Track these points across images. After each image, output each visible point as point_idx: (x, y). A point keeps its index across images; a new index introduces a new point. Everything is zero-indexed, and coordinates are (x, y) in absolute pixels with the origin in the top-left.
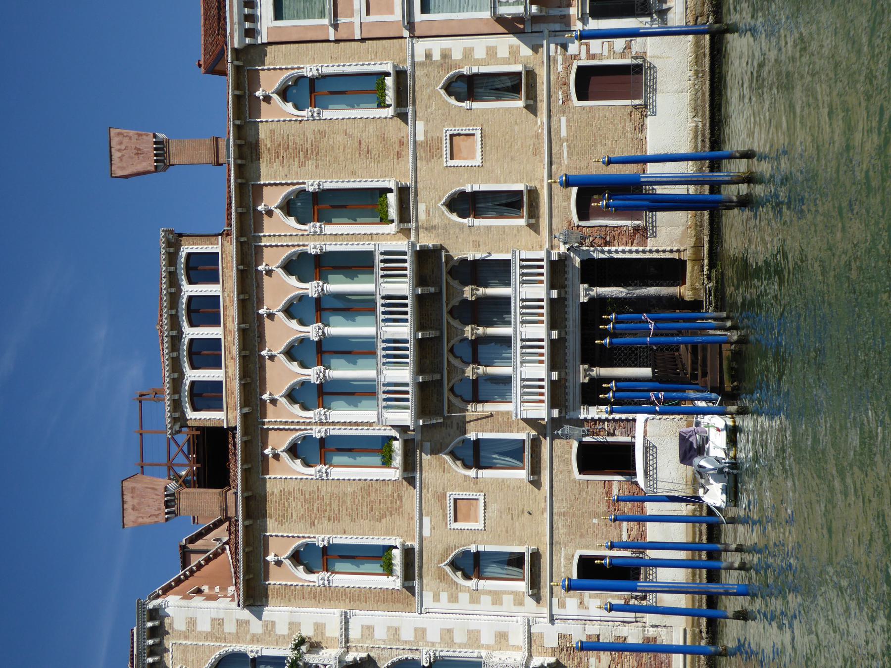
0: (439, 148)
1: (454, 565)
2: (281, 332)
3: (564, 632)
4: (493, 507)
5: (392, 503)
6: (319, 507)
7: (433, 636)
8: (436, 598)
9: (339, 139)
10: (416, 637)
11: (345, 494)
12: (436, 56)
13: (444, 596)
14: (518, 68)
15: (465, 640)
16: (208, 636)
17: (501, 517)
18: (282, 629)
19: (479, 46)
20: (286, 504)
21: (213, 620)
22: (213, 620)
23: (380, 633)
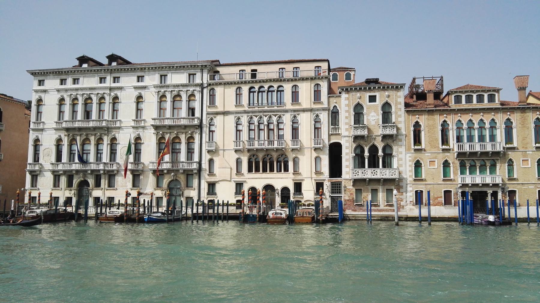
1: (418, 161)
2: (476, 119)
6: (431, 128)
7: (400, 156)
8: (410, 157)
13: (410, 159)
18: (400, 119)
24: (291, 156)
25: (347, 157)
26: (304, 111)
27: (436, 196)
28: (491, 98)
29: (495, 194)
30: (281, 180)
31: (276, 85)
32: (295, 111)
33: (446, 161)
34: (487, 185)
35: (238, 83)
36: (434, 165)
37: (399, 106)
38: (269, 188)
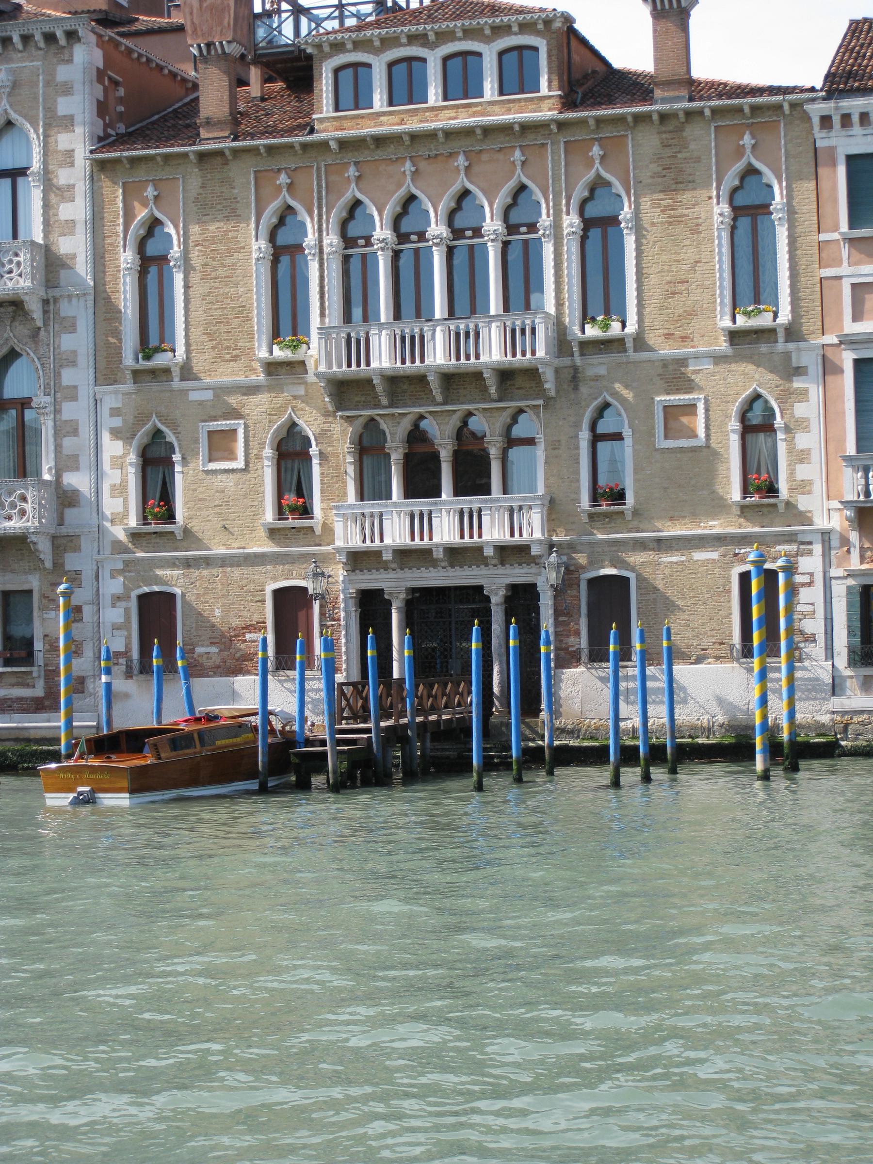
0: (678, 391)
3: (83, 577)
4: (229, 481)
5: (228, 348)
7: (69, 411)
8: (115, 412)
9: (690, 254)
10: (68, 387)
11: (236, 285)
13: (117, 422)
17: (217, 492)
20: (219, 207)
23: (67, 342)
29: (522, 600)
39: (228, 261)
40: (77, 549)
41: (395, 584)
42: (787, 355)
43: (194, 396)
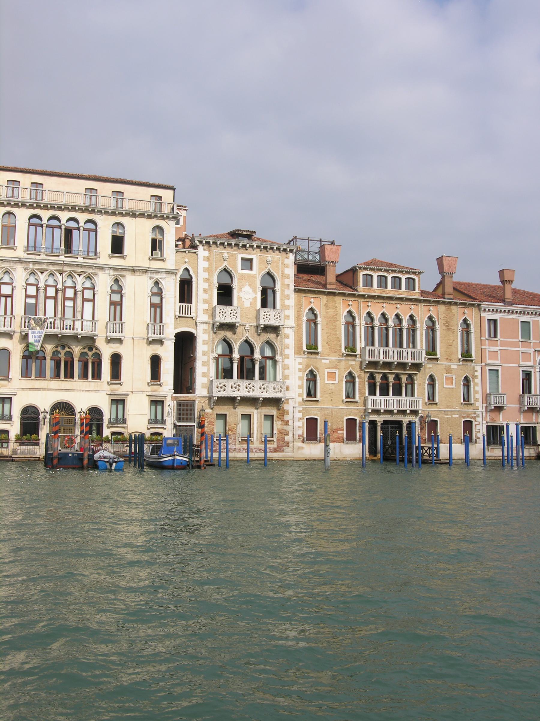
1: (311, 372)
2: (391, 311)
6: (331, 320)
7: (287, 362)
8: (300, 364)
9: (452, 338)
11: (336, 331)
12: (476, 374)
13: (301, 367)
14: (472, 402)
15: (286, 374)
16: (283, 272)
18: (287, 302)
19: (479, 388)
21: (289, 275)
22: (289, 275)
23: (287, 341)
24: (107, 352)
25: (205, 358)
26: (133, 270)
27: (335, 427)
28: (411, 283)
30: (85, 395)
31: (82, 217)
32: (116, 269)
33: (350, 373)
34: (404, 412)
35: (9, 205)
36: (334, 378)
37: (286, 281)
38: (64, 408)
39: (334, 324)
40: (288, 403)
41: (380, 419)
42: (474, 367)
43: (323, 361)
